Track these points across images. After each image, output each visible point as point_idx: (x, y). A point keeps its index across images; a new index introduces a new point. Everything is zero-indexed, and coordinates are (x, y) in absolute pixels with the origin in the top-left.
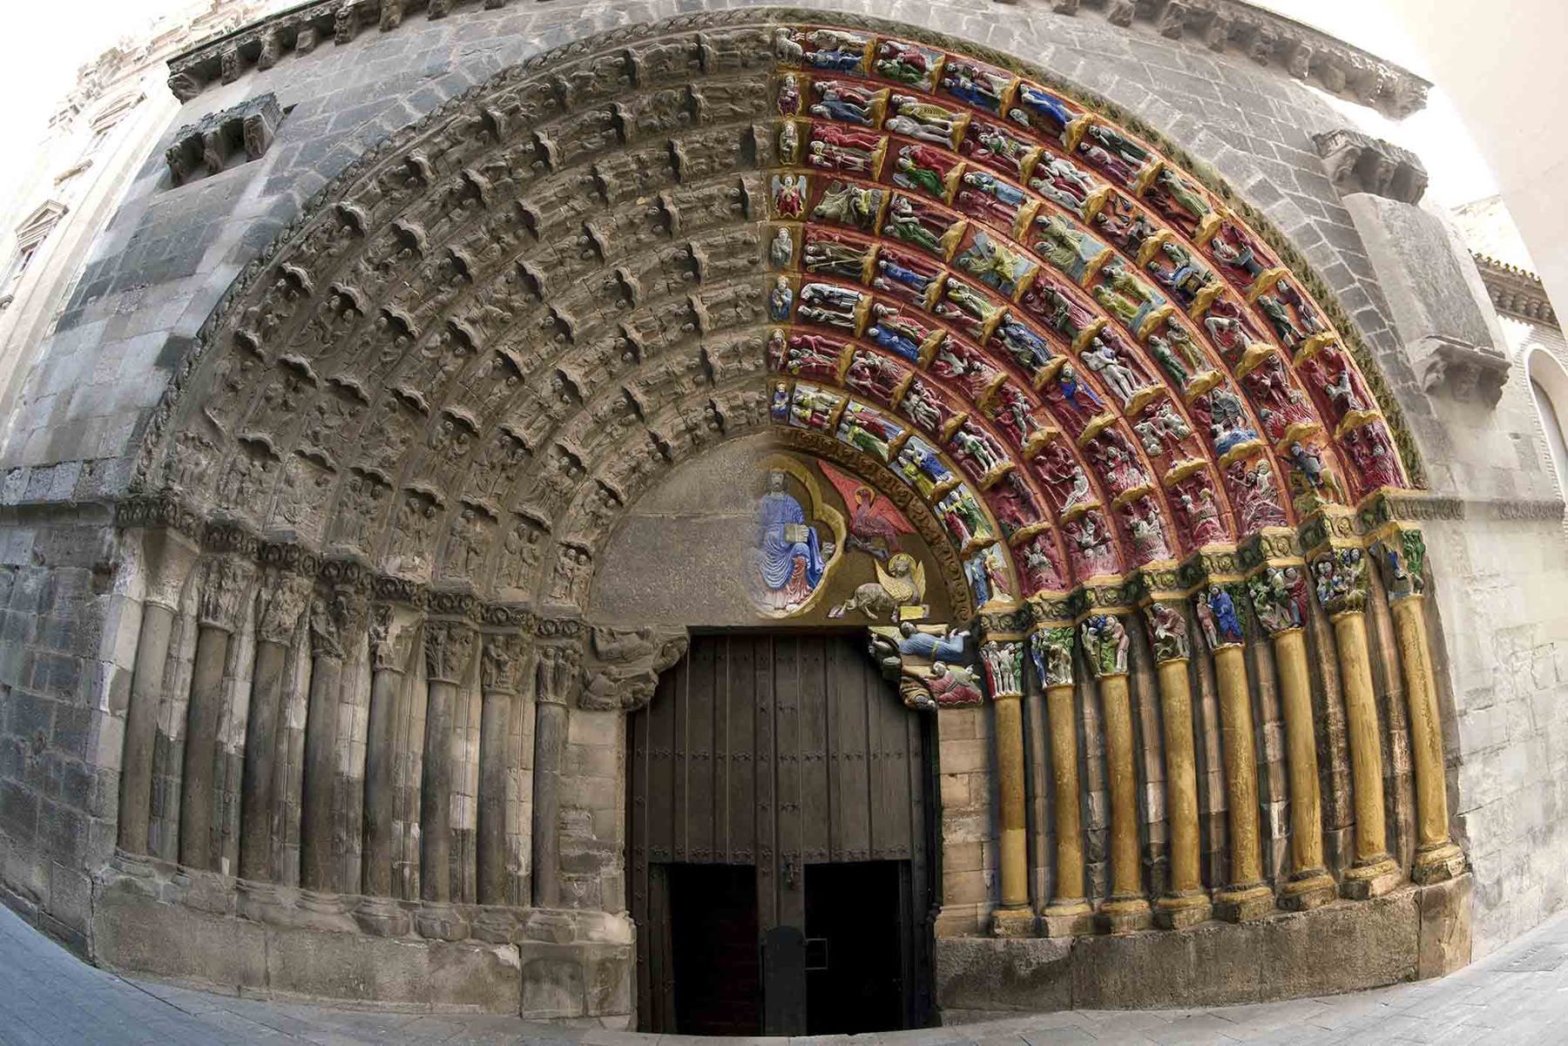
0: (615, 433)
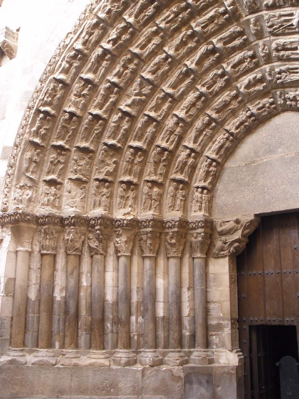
0: (208, 134)
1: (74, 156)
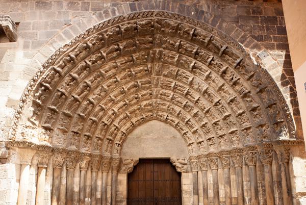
1: (61, 116)
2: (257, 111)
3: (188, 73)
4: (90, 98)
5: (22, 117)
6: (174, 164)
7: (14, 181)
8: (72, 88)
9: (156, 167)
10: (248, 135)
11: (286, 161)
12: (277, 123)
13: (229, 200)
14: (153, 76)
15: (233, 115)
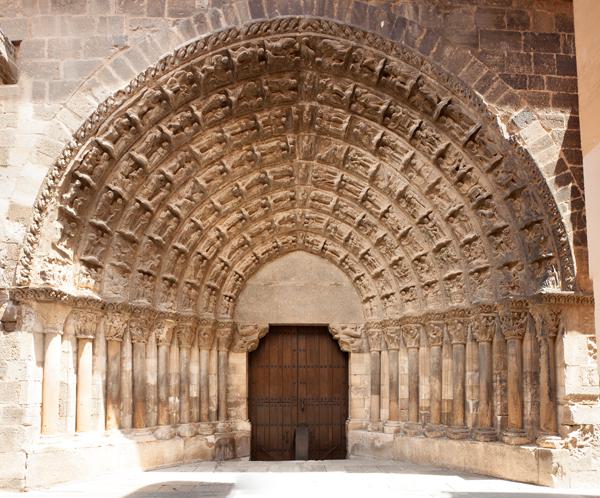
1: (116, 240)
2: (503, 236)
3: (369, 156)
4: (173, 206)
5: (41, 241)
6: (336, 336)
7: (32, 364)
8: (136, 184)
9: (302, 342)
10: (481, 282)
11: (551, 335)
12: (540, 261)
13: (437, 406)
14: (297, 160)
15: (454, 242)
